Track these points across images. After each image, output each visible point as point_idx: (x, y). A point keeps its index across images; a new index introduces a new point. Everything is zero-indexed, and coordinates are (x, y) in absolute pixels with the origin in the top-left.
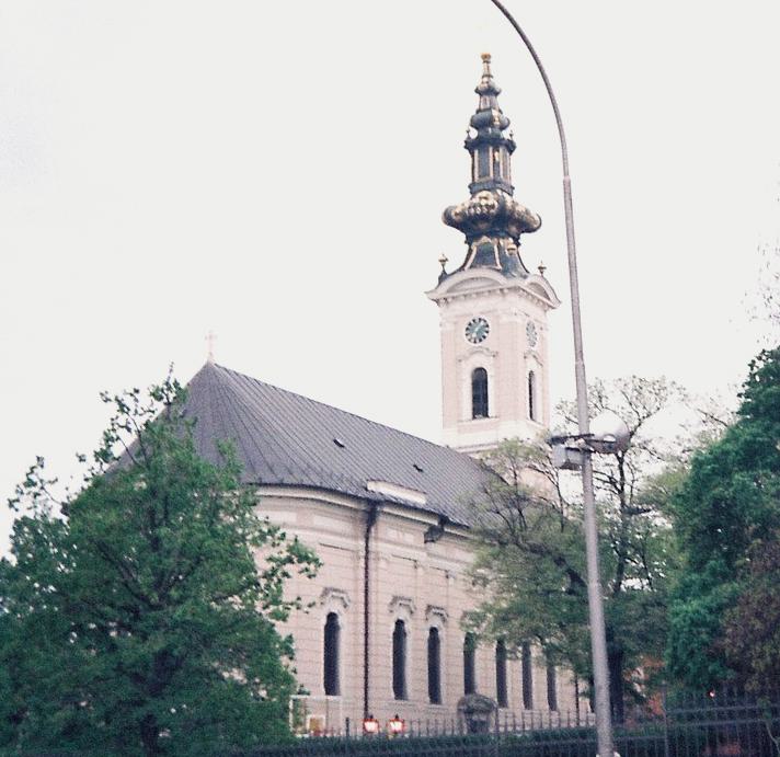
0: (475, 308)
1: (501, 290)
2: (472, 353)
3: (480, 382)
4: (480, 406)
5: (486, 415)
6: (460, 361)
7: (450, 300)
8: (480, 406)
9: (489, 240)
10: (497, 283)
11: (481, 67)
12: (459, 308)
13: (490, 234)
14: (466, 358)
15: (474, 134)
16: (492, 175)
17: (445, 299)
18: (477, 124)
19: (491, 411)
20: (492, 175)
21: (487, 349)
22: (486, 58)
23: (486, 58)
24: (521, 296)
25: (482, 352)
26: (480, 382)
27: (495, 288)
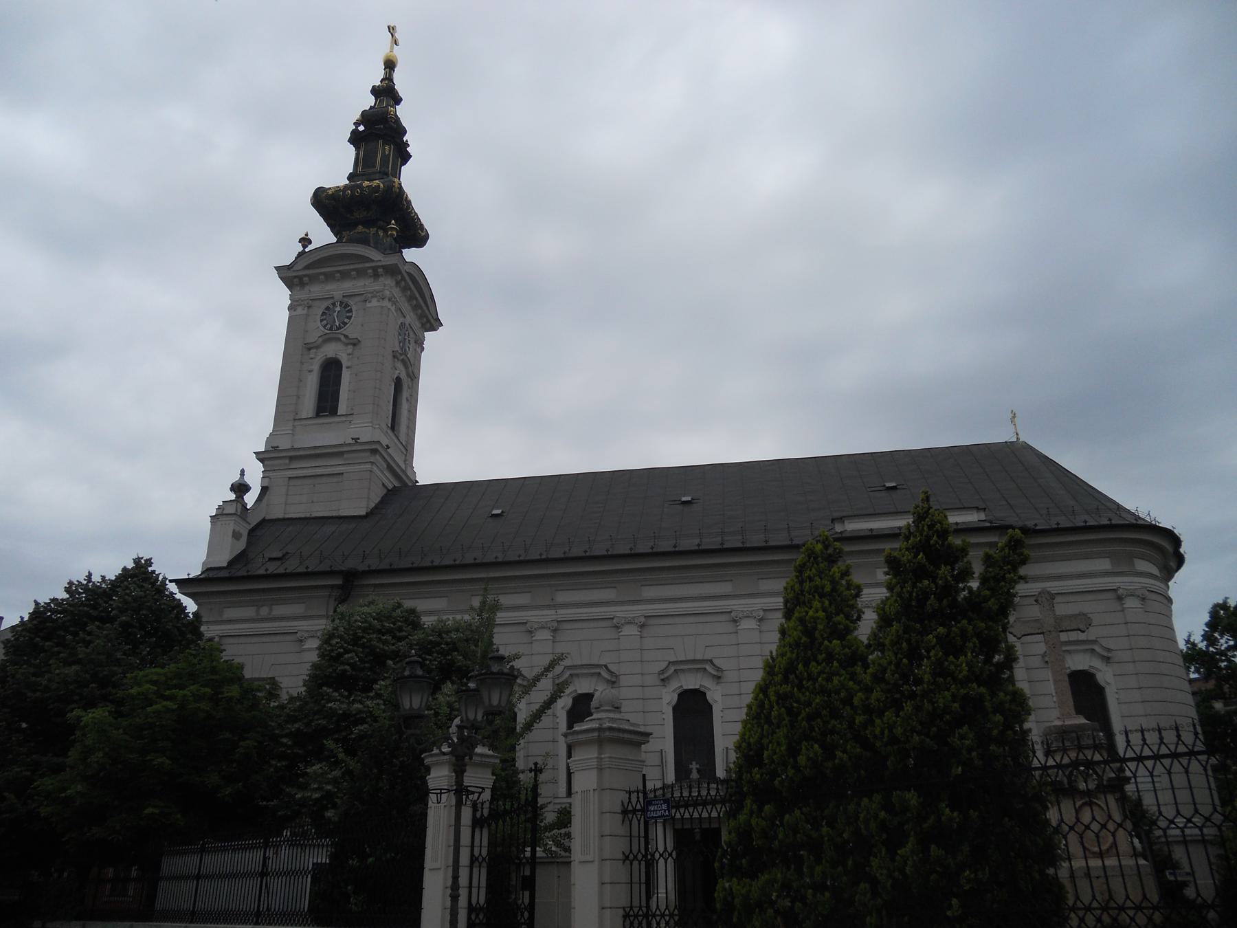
0: (337, 289)
1: (375, 269)
2: (325, 341)
3: (331, 372)
4: (327, 404)
5: (333, 411)
6: (309, 349)
7: (306, 279)
8: (327, 404)
9: (367, 230)
10: (367, 259)
11: (381, 73)
12: (316, 290)
13: (368, 223)
14: (317, 347)
15: (361, 128)
16: (378, 167)
17: (300, 278)
18: (366, 118)
19: (342, 408)
20: (378, 167)
21: (346, 336)
22: (390, 65)
23: (390, 65)
24: (398, 283)
25: (339, 339)
26: (331, 372)
27: (367, 265)
